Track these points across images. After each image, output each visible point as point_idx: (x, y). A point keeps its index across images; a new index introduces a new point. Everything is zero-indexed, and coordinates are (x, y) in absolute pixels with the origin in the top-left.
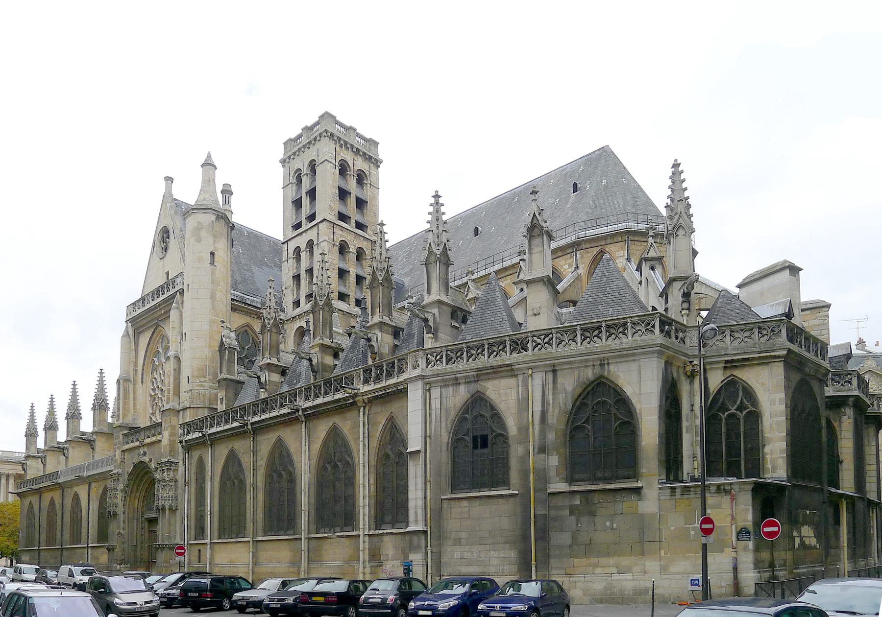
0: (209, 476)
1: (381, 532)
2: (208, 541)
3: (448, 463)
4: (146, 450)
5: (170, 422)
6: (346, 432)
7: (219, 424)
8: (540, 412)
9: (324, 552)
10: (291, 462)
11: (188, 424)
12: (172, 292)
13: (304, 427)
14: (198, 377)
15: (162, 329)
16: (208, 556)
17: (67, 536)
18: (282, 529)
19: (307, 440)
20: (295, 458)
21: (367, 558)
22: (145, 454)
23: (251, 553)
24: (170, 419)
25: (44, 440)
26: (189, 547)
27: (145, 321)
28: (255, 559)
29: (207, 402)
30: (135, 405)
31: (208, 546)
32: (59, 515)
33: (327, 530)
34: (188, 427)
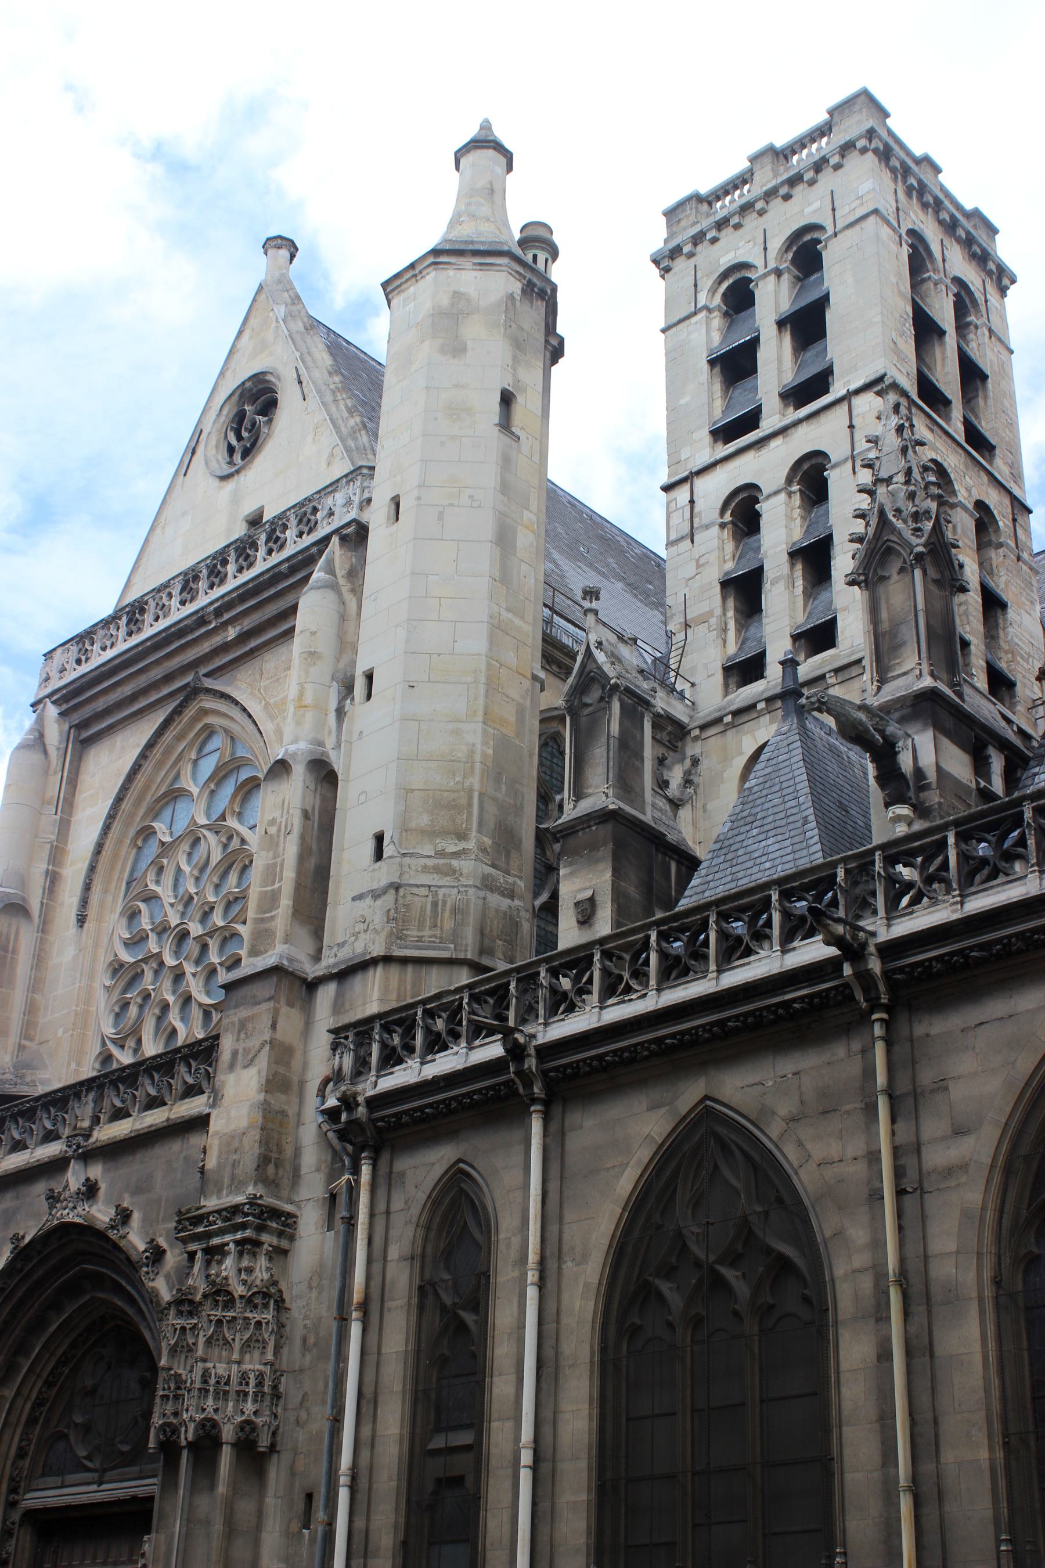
5: (274, 1026)
12: (294, 544)
14: (430, 833)
24: (276, 1013)
29: (469, 935)
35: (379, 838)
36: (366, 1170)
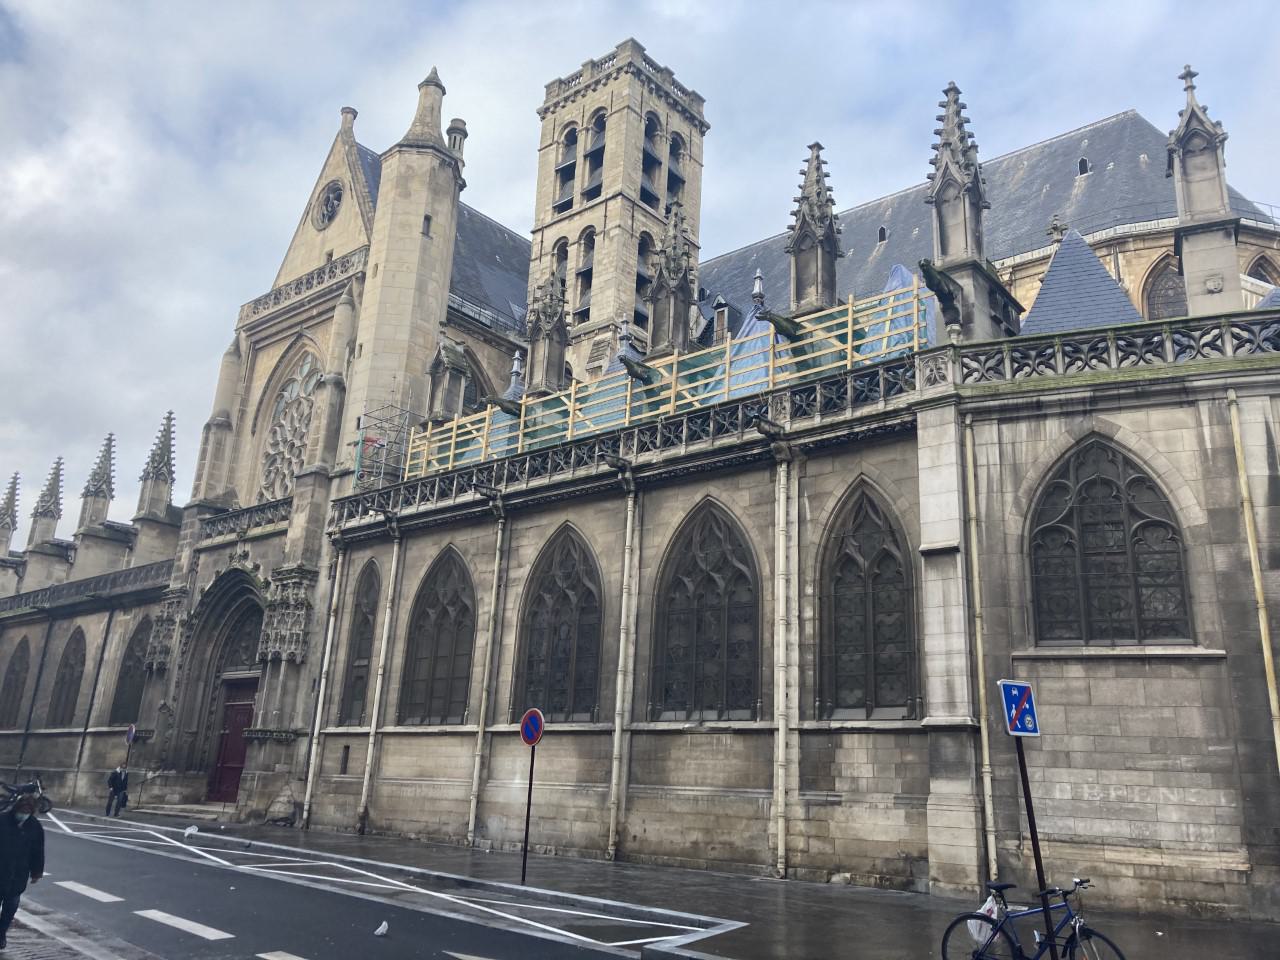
0: (390, 598)
1: (835, 725)
2: (372, 729)
3: (1024, 579)
4: (248, 547)
6: (738, 512)
7: (424, 498)
8: (1266, 481)
9: (671, 764)
10: (593, 572)
11: (354, 501)
12: (340, 277)
13: (630, 503)
15: (306, 341)
16: (369, 761)
17: (42, 710)
18: (561, 710)
19: (637, 533)
20: (603, 563)
21: (795, 782)
22: (245, 556)
23: (478, 759)
25: (28, 533)
26: (322, 740)
27: (274, 330)
28: (485, 771)
30: (232, 471)
31: (371, 739)
32: (34, 670)
33: (682, 714)
34: (350, 505)
35: (359, 419)
36: (340, 558)
